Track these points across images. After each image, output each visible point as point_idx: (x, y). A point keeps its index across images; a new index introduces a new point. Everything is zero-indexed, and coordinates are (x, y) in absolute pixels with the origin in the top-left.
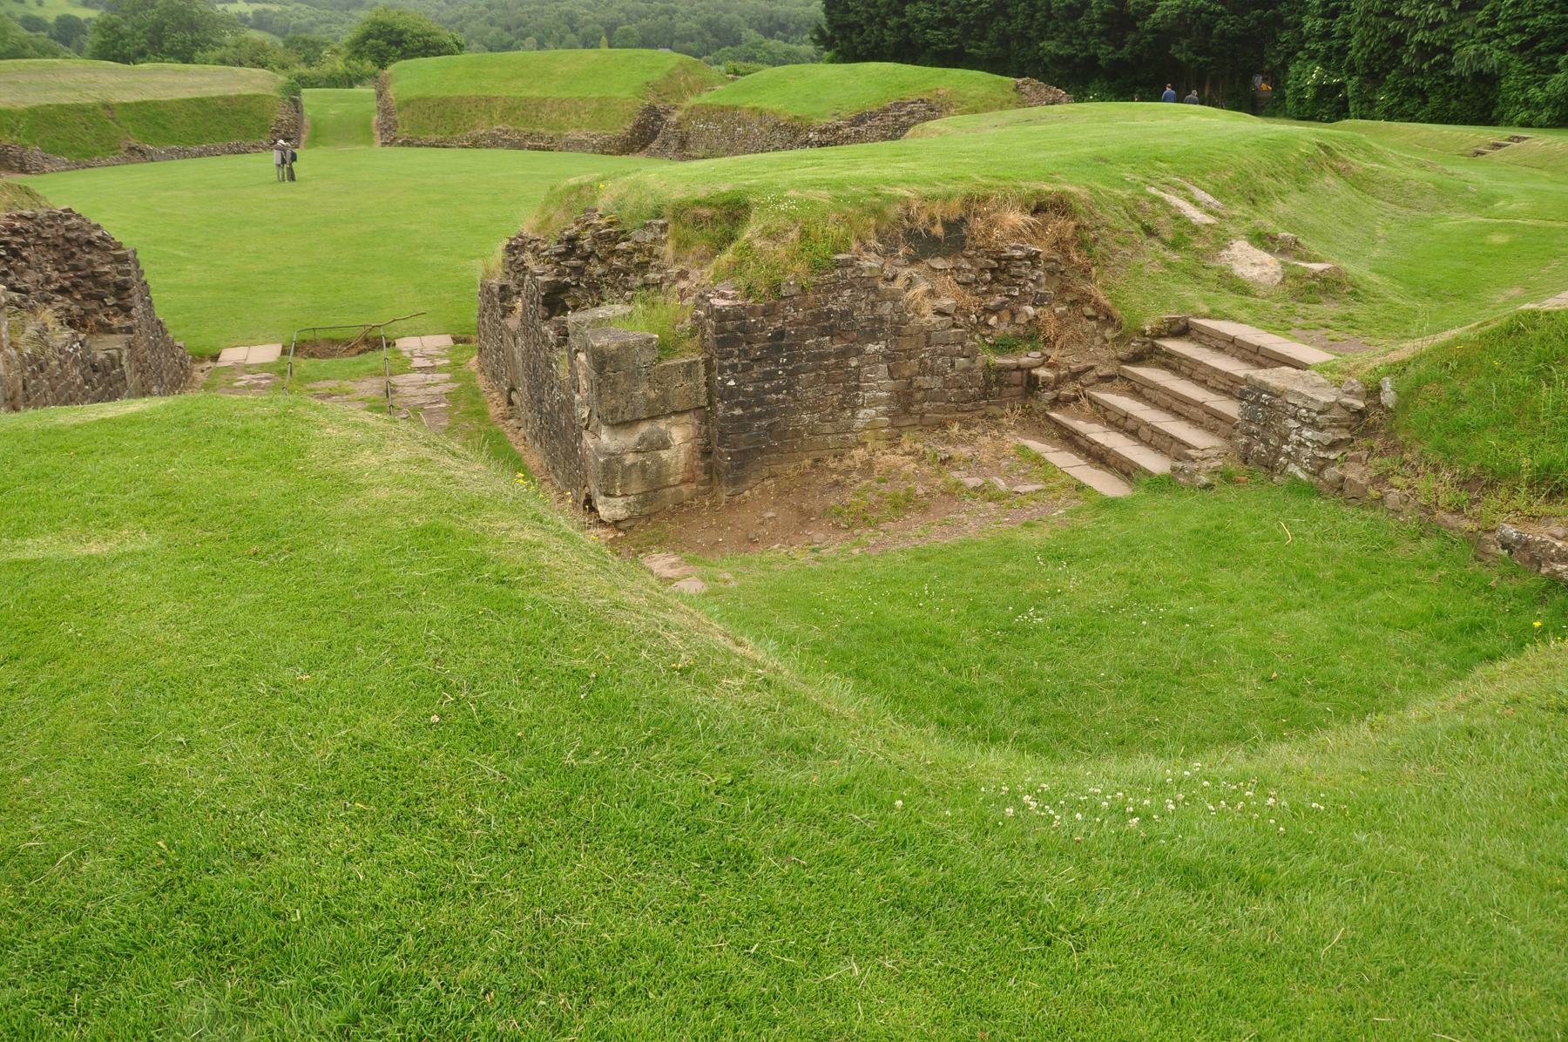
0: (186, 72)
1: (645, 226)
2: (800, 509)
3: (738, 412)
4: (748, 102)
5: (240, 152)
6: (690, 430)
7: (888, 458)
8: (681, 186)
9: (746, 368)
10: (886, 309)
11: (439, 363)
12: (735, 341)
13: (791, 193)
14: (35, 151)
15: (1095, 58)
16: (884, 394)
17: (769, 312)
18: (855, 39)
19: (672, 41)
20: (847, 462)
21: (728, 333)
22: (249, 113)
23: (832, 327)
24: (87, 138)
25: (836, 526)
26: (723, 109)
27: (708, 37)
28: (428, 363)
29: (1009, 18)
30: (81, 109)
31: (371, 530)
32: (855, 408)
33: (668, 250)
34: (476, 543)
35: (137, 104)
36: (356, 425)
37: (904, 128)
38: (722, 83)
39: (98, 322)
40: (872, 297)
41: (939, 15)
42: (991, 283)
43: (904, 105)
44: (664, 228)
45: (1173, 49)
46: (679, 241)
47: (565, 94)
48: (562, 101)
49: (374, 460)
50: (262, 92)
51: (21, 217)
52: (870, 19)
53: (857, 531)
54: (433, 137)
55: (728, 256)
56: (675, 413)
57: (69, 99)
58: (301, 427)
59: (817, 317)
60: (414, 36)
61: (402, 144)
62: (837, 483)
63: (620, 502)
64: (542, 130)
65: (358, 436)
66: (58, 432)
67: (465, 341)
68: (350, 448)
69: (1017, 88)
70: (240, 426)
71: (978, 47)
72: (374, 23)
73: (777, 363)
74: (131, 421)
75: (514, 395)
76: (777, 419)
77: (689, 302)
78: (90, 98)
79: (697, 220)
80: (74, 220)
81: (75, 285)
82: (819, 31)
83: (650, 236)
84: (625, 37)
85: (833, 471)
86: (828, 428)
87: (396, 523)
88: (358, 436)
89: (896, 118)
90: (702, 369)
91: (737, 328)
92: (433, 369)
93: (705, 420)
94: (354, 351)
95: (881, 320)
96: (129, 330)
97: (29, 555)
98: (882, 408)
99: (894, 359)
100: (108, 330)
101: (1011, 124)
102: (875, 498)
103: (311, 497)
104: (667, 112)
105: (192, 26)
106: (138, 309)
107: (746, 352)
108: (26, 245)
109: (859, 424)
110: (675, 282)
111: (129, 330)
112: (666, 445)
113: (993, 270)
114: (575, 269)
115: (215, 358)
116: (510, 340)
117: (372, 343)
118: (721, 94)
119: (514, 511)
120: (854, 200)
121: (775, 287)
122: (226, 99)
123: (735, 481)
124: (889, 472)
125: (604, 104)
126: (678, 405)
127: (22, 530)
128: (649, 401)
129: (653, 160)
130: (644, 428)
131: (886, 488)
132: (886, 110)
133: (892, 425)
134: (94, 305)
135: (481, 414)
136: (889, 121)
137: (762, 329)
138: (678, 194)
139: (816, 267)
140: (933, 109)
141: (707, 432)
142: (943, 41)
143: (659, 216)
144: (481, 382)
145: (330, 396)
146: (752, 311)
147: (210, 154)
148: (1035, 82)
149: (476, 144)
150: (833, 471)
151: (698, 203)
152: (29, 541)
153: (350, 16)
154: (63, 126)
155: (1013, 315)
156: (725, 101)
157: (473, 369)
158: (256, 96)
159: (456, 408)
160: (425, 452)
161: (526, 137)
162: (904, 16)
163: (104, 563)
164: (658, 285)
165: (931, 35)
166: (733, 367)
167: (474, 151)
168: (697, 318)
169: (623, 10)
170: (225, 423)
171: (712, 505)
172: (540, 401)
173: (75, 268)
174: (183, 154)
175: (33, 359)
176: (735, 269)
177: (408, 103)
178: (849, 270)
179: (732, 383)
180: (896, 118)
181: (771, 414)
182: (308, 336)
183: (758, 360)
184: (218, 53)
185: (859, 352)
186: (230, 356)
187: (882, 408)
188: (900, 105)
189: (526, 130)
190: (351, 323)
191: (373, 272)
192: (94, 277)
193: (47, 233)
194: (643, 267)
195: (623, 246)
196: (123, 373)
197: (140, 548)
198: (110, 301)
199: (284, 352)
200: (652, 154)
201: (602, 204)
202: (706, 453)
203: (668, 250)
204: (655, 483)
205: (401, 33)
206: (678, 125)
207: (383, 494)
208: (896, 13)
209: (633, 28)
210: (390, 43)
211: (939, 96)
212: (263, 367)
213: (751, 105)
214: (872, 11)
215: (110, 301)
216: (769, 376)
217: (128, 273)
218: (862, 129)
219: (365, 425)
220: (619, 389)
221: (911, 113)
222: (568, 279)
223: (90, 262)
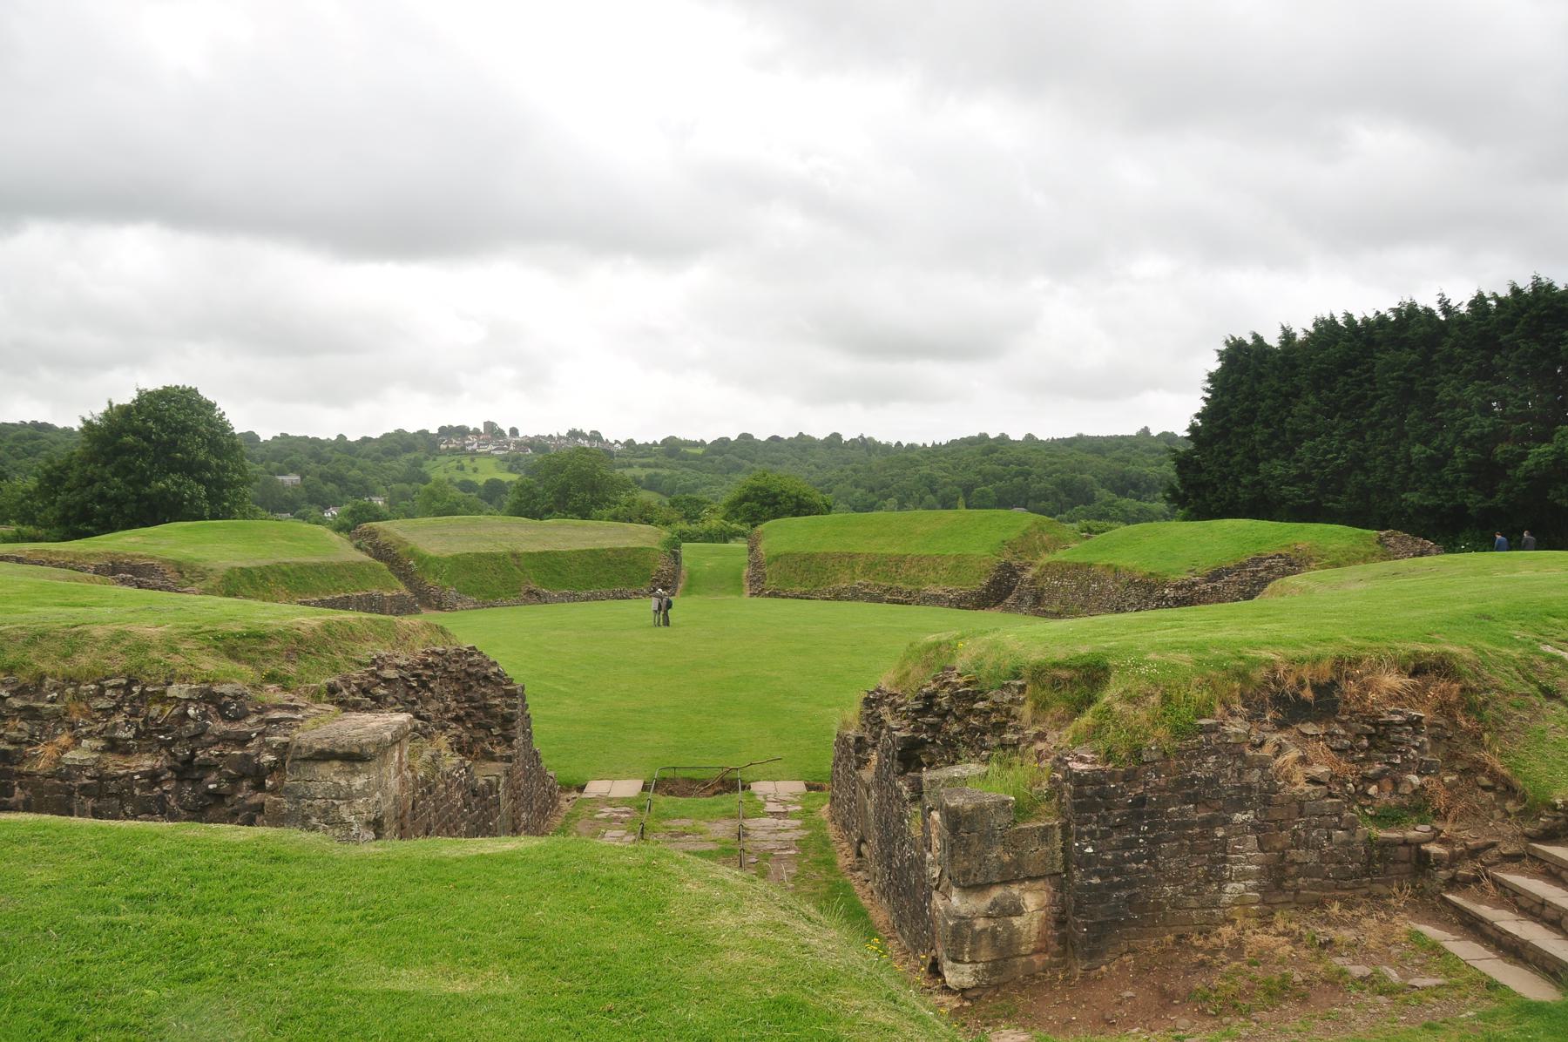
0: (584, 527)
1: (1003, 687)
2: (1161, 989)
3: (1095, 880)
4: (1101, 559)
6: (1044, 897)
7: (1260, 939)
8: (1040, 648)
9: (1106, 835)
10: (1254, 776)
11: (790, 809)
12: (1094, 807)
13: (1152, 656)
14: (452, 591)
15: (1464, 507)
16: (1254, 867)
17: (1130, 778)
20: (1214, 940)
21: (1087, 798)
22: (634, 563)
23: (1196, 794)
25: (1203, 1012)
26: (1077, 566)
27: (1062, 496)
28: (780, 809)
29: (1367, 472)
30: (493, 557)
31: (724, 997)
32: (1222, 881)
33: (1026, 711)
34: (829, 1022)
35: (540, 554)
36: (716, 883)
37: (1264, 583)
38: (1076, 541)
39: (483, 750)
40: (1239, 763)
41: (1294, 472)
42: (1368, 749)
43: (1262, 560)
44: (1022, 689)
45: (1552, 494)
46: (1037, 702)
47: (925, 552)
49: (731, 921)
51: (434, 652)
52: (1224, 478)
53: (1226, 1020)
54: (798, 590)
55: (1086, 719)
56: (1029, 878)
57: (485, 548)
58: (663, 880)
59: (1180, 784)
61: (769, 595)
62: (1202, 963)
63: (968, 968)
64: (901, 585)
65: (717, 894)
66: (440, 863)
67: (818, 788)
68: (708, 906)
69: (1381, 541)
70: (606, 874)
71: (1336, 501)
73: (1138, 831)
74: (507, 859)
75: (863, 847)
76: (1138, 890)
77: (1047, 764)
78: (502, 548)
79: (1056, 683)
80: (476, 657)
81: (468, 715)
82: (1172, 490)
83: (1007, 697)
84: (982, 497)
85: (1199, 949)
86: (1193, 902)
87: (749, 992)
88: (717, 894)
89: (1254, 573)
90: (1058, 836)
91: (1098, 793)
92: (785, 814)
93: (1060, 887)
94: (710, 792)
95: (1249, 788)
96: (509, 759)
97: (401, 986)
98: (1251, 883)
99: (1264, 830)
100: (490, 757)
101: (1376, 578)
102: (1245, 983)
103: (667, 956)
104: (1023, 569)
105: (594, 488)
106: (519, 740)
107: (1105, 819)
108: (433, 678)
109: (1226, 899)
110: (1032, 743)
111: (509, 759)
112: (1018, 911)
113: (1369, 736)
114: (931, 725)
115: (581, 789)
116: (863, 792)
117: (728, 784)
118: (1076, 552)
119: (868, 989)
120: (1218, 664)
121: (1136, 752)
122: (615, 551)
123: (1091, 955)
124: (1261, 954)
125: (961, 562)
126: (1031, 870)
127: (399, 960)
128: (1002, 865)
129: (1008, 616)
130: (997, 892)
131: (1258, 972)
132: (1243, 566)
133: (1263, 902)
134: (481, 734)
135: (830, 864)
136: (1247, 576)
137: (1123, 795)
138: (1036, 656)
139: (1179, 732)
140: (1293, 564)
141: (1062, 900)
142: (1299, 496)
143: (1017, 676)
144: (832, 831)
145: (684, 834)
146: (1112, 776)
147: (596, 599)
148: (1400, 534)
149: (837, 596)
150: (1199, 949)
151: (1056, 665)
152: (404, 972)
155: (1396, 784)
156: (1080, 558)
157: (825, 817)
159: (805, 856)
160: (781, 917)
162: (1257, 473)
163: (467, 1003)
164: (1015, 746)
165: (1286, 490)
166: (1091, 833)
168: (1055, 780)
169: (979, 473)
170: (592, 869)
171: (1065, 979)
172: (891, 856)
173: (470, 700)
174: (573, 598)
175: (425, 782)
176: (1095, 732)
177: (776, 558)
178: (1214, 736)
179: (1090, 850)
180: (1254, 573)
181: (1131, 885)
182: (669, 774)
183: (1118, 826)
185: (1226, 822)
186: (595, 788)
187: (1251, 883)
188: (1258, 560)
189: (887, 584)
190: (710, 764)
191: (734, 716)
192: (486, 708)
193: (452, 668)
194: (1000, 727)
195: (980, 705)
196: (498, 798)
197: (502, 991)
198: (496, 731)
199: (645, 788)
200: (1007, 609)
201: (961, 663)
202: (1061, 922)
203: (1026, 711)
204: (1005, 950)
205: (775, 496)
206: (1033, 582)
207: (738, 959)
208: (1249, 471)
209: (989, 489)
210: (763, 504)
211: (1297, 550)
212: (624, 801)
213: (1106, 562)
215: (496, 731)
216: (1129, 845)
217: (515, 706)
218: (1219, 584)
219: (724, 883)
220: (972, 850)
221: (1269, 568)
222: (924, 736)
223: (484, 695)
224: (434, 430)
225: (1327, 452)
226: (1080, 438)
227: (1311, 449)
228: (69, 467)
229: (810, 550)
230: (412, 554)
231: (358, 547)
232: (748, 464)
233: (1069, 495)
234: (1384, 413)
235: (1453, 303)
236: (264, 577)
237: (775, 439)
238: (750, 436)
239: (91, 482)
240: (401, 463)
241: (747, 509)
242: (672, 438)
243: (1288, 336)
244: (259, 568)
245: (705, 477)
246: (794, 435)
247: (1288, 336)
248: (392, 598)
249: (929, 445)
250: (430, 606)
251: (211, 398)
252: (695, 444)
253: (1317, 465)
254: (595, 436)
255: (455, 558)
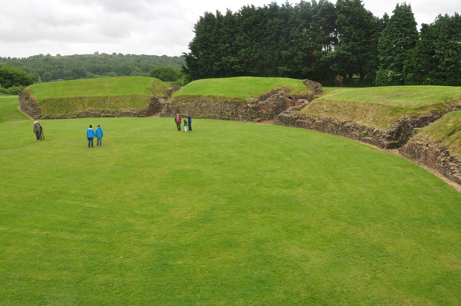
15: (301, 71)
18: (200, 70)
19: (63, 76)
27: (75, 75)
29: (263, 60)
45: (331, 67)
47: (115, 95)
48: (115, 97)
54: (59, 115)
60: (18, 75)
61: (45, 118)
64: (109, 109)
71: (253, 70)
82: (184, 67)
84: (47, 76)
125: (134, 98)
142: (240, 68)
148: (309, 81)
161: (102, 112)
162: (221, 61)
167: (78, 119)
169: (45, 67)
177: (44, 101)
189: (102, 109)
200: (162, 116)
205: (11, 75)
209: (49, 73)
214: (207, 60)
225: (250, 53)
226: (76, 55)
227: (244, 52)
229: (59, 97)
233: (77, 74)
234: (271, 39)
235: (290, 4)
243: (229, 13)
247: (229, 13)
249: (21, 58)
253: (246, 57)
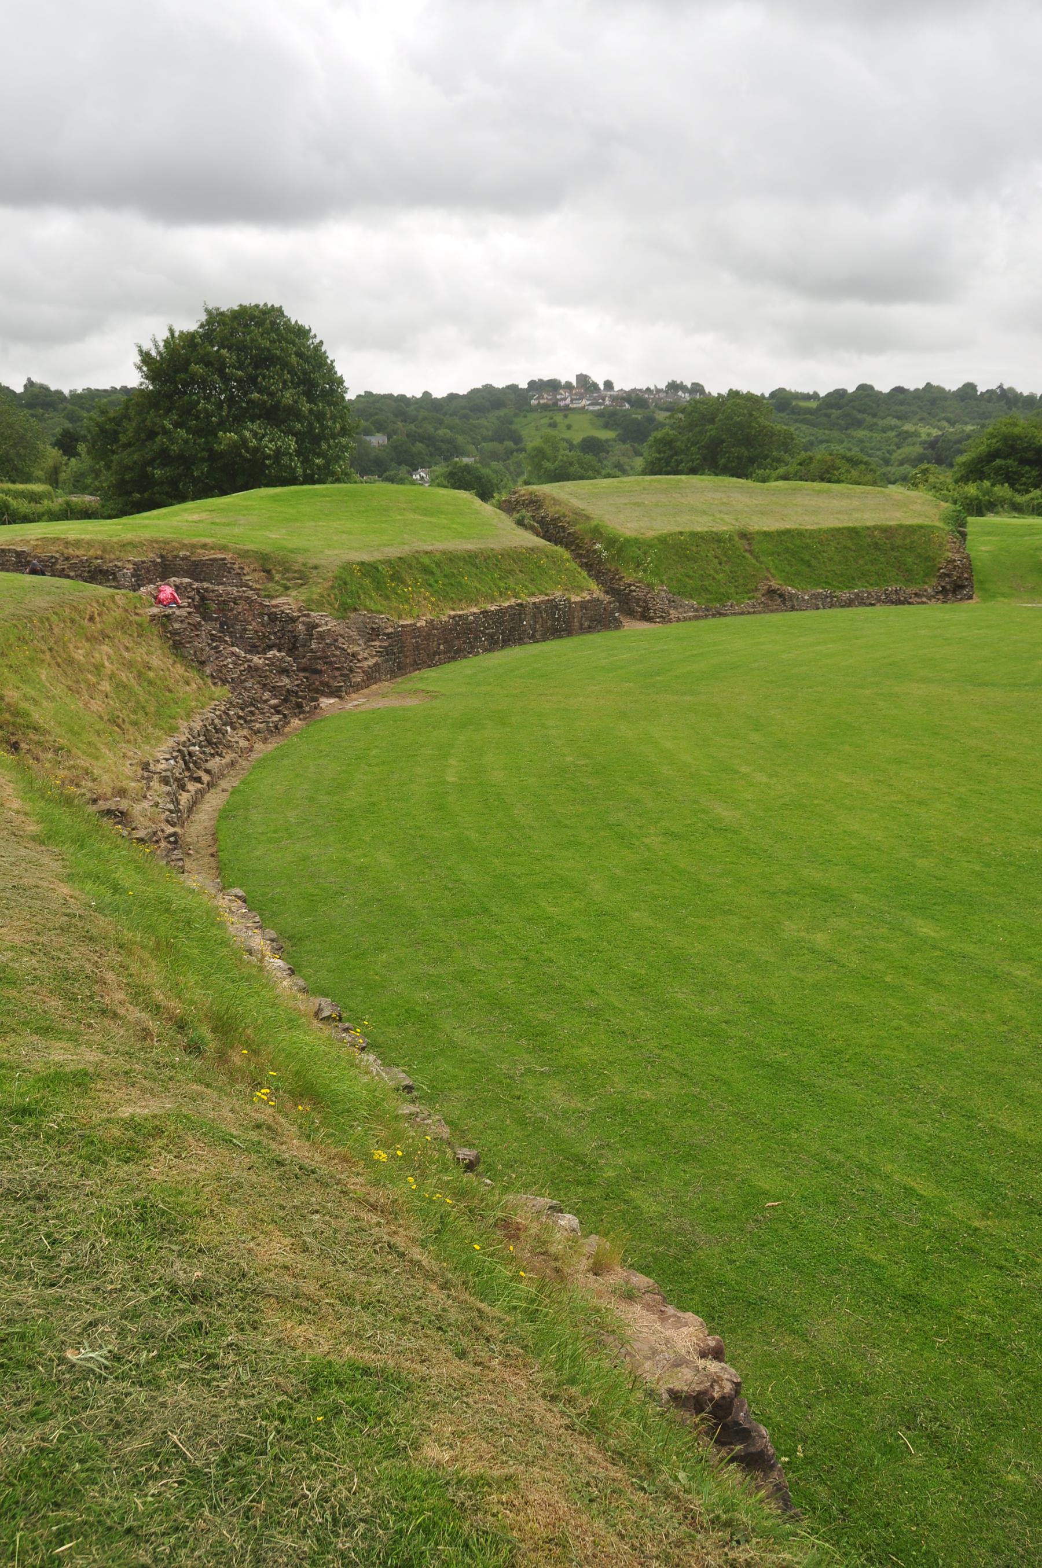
0: (828, 492)
5: (899, 602)
14: (661, 590)
22: (911, 549)
24: (720, 576)
30: (716, 538)
50: (927, 522)
57: (702, 525)
72: (1005, 438)
78: (725, 525)
105: (748, 441)
122: (886, 531)
147: (863, 603)
153: (849, 436)
154: (695, 560)
158: (921, 527)
174: (830, 602)
184: (781, 471)
224: (524, 385)
228: (126, 416)
230: (597, 532)
231: (520, 523)
232: (868, 419)
236: (397, 577)
237: (899, 390)
238: (871, 388)
239: (152, 435)
240: (488, 422)
241: (1000, 468)
242: (781, 390)
244: (388, 562)
245: (821, 433)
246: (921, 386)
248: (583, 605)
250: (630, 613)
251: (304, 322)
252: (807, 397)
254: (697, 388)
255: (662, 540)
